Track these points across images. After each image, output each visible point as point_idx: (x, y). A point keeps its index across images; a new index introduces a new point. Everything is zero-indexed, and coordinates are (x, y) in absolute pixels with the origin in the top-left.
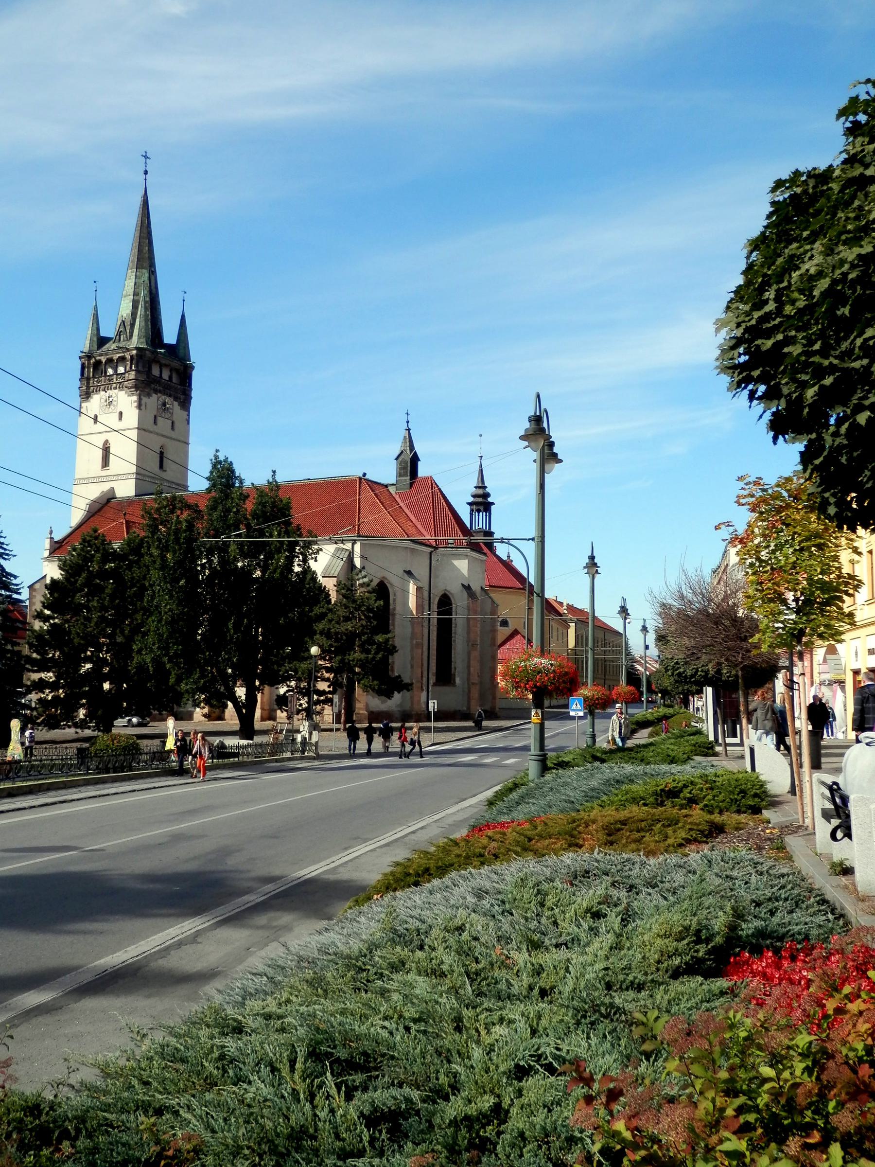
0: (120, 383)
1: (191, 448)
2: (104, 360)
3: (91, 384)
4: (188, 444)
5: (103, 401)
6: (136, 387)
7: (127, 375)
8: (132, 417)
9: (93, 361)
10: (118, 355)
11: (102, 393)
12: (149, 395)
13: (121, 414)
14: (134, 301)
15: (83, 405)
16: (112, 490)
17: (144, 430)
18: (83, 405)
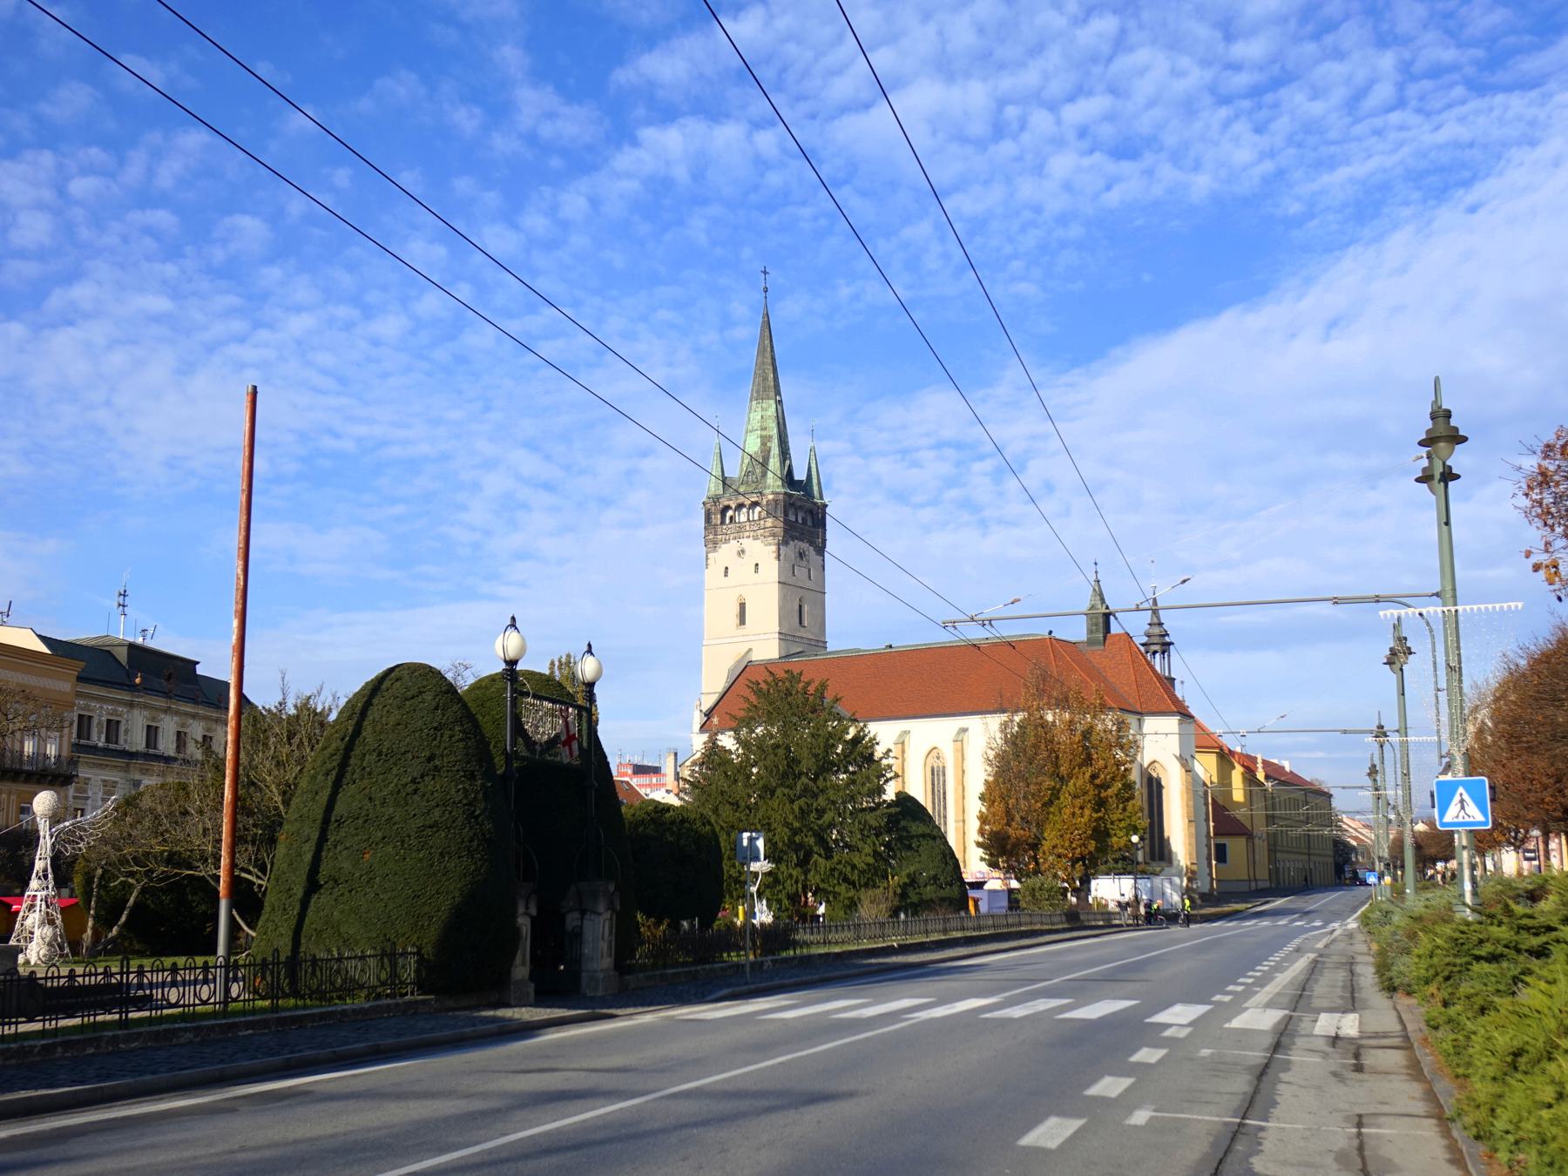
1: (827, 596)
6: (774, 535)
7: (762, 522)
8: (771, 569)
11: (733, 542)
12: (785, 542)
13: (757, 565)
14: (761, 437)
16: (750, 650)
17: (784, 583)
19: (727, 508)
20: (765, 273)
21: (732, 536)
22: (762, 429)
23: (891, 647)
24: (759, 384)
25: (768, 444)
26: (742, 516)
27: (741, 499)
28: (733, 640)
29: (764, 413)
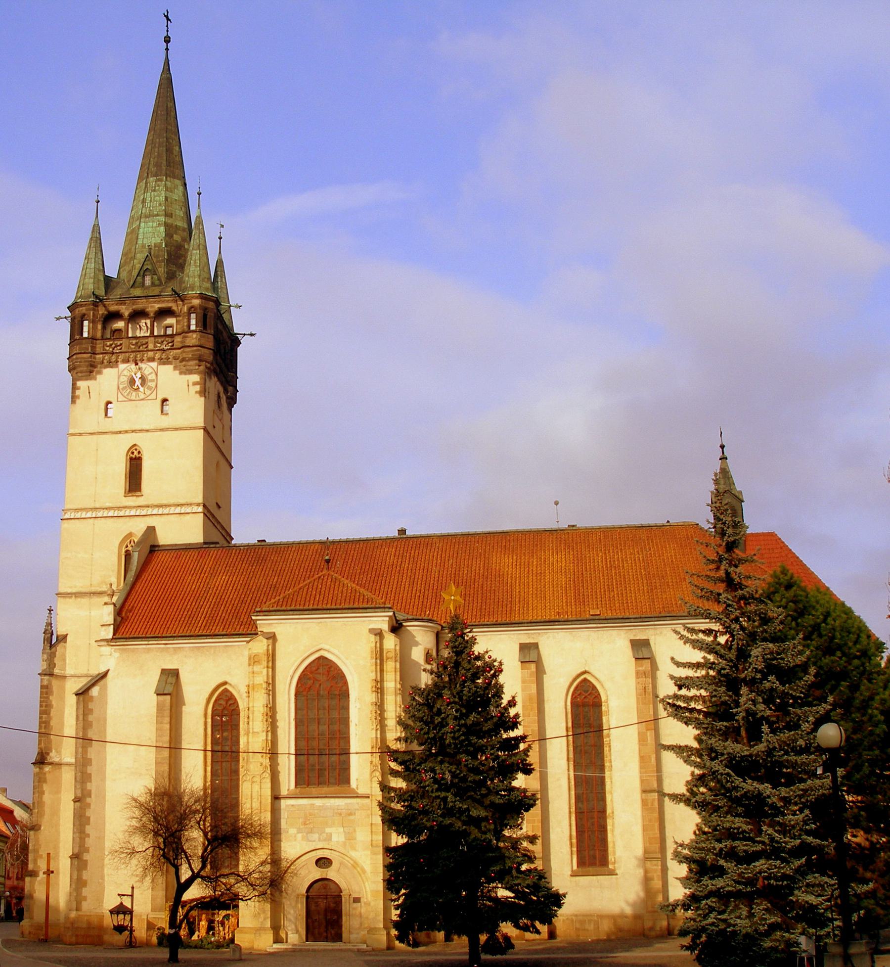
0: (163, 350)
2: (126, 311)
3: (98, 350)
4: (232, 467)
5: (124, 379)
6: (200, 360)
7: (178, 339)
9: (102, 311)
10: (157, 306)
14: (166, 225)
15: (79, 383)
16: (151, 530)
18: (79, 383)
19: (117, 316)
20: (168, 19)
21: (121, 357)
22: (168, 215)
23: (402, 531)
24: (159, 156)
25: (176, 237)
26: (143, 328)
27: (140, 305)
28: (122, 514)
29: (169, 194)
